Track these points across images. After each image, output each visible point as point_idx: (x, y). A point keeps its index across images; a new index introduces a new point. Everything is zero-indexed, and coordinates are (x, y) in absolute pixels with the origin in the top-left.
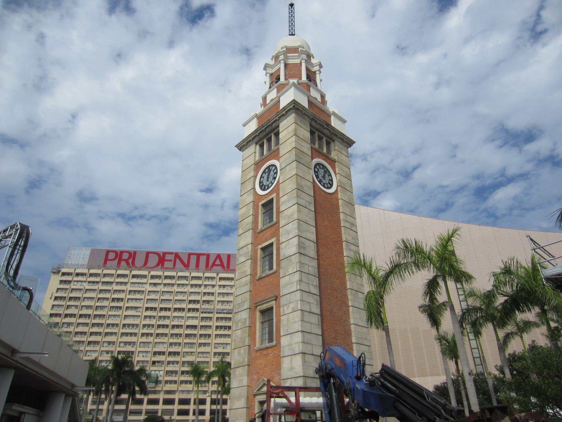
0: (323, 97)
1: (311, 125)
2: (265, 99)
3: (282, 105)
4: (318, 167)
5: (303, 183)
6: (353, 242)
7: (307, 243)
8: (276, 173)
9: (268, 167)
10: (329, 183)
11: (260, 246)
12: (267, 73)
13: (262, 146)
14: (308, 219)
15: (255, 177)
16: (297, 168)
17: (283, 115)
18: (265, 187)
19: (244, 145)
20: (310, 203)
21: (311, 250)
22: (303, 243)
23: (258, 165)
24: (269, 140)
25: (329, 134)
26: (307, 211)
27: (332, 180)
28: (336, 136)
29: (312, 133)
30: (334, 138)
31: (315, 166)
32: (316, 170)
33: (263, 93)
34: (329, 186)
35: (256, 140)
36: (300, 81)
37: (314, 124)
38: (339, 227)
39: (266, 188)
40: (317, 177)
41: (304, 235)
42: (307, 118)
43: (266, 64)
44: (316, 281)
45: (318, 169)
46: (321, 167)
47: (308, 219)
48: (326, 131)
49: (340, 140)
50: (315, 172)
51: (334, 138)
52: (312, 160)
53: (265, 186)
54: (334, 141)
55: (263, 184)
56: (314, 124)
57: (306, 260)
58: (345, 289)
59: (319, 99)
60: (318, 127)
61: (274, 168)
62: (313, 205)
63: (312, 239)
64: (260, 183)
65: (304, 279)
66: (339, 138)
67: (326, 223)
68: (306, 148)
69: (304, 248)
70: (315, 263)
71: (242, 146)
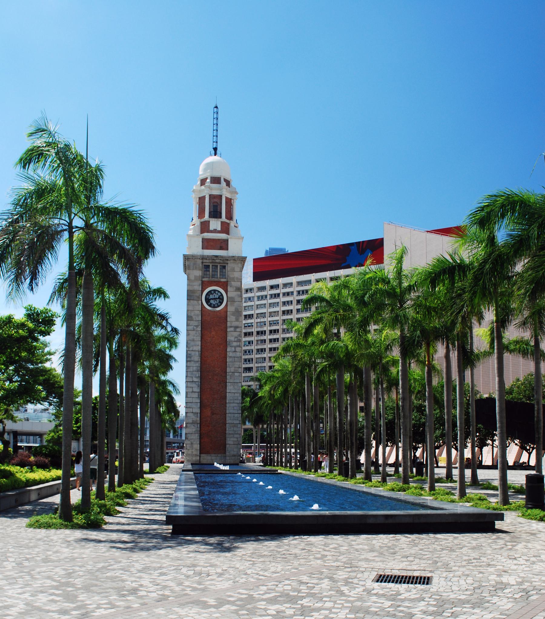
5: (192, 314)
6: (236, 339)
7: (193, 353)
10: (220, 302)
14: (195, 338)
16: (188, 305)
20: (197, 326)
21: (196, 357)
22: (190, 354)
25: (221, 262)
26: (194, 332)
27: (223, 299)
30: (227, 262)
32: (208, 297)
34: (219, 304)
37: (205, 261)
38: (226, 332)
41: (191, 349)
42: (199, 260)
44: (198, 374)
47: (195, 338)
48: (217, 261)
49: (232, 261)
51: (227, 262)
56: (205, 261)
57: (192, 364)
58: (226, 372)
59: (220, 229)
60: (211, 261)
62: (200, 327)
63: (197, 350)
65: (189, 375)
67: (213, 333)
68: (197, 287)
69: (190, 357)
70: (198, 364)
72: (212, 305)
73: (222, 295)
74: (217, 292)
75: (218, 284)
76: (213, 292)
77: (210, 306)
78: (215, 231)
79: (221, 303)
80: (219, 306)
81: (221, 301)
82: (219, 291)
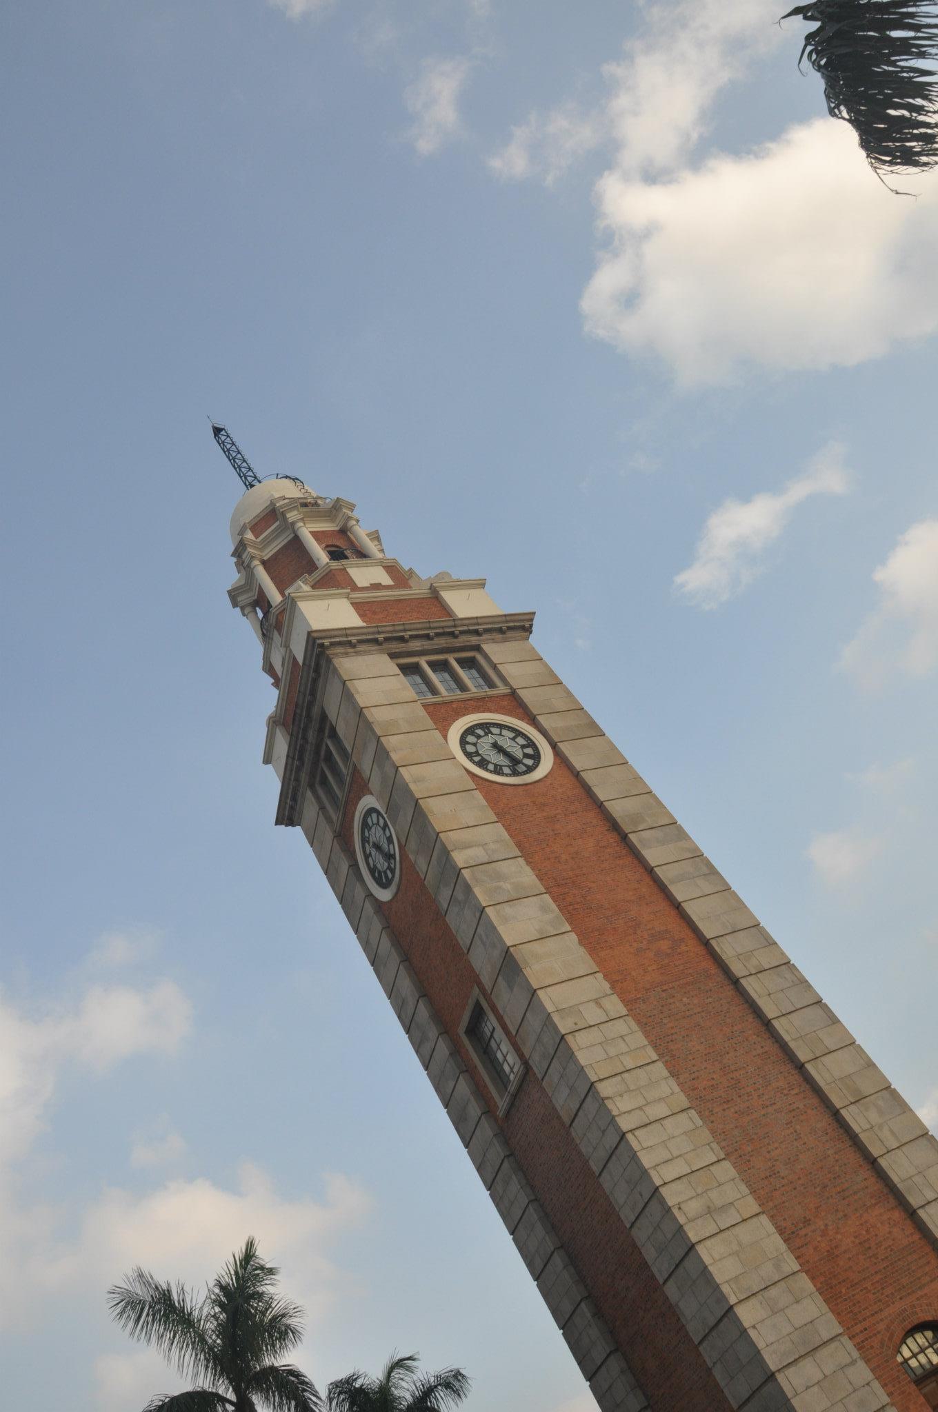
0: (392, 569)
1: (393, 656)
2: (269, 669)
3: (300, 661)
4: (471, 739)
8: (386, 825)
9: (365, 825)
11: (461, 1030)
12: (242, 609)
13: (324, 782)
15: (354, 865)
17: (315, 681)
18: (387, 877)
19: (292, 808)
23: (343, 836)
24: (329, 757)
27: (531, 744)
28: (477, 633)
29: (409, 670)
30: (473, 639)
31: (463, 742)
32: (470, 749)
33: (260, 662)
34: (530, 762)
35: (304, 777)
36: (316, 575)
37: (397, 647)
39: (390, 875)
40: (483, 764)
43: (229, 592)
45: (475, 744)
46: (480, 732)
50: (469, 755)
51: (473, 639)
52: (445, 737)
53: (385, 873)
54: (478, 648)
55: (380, 872)
59: (387, 580)
61: (374, 816)
64: (372, 871)
66: (487, 631)
71: (287, 815)
72: (506, 770)
73: (518, 733)
74: (495, 730)
75: (480, 704)
76: (480, 732)
77: (498, 770)
78: (377, 587)
79: (536, 757)
80: (530, 769)
81: (529, 751)
82: (501, 726)
